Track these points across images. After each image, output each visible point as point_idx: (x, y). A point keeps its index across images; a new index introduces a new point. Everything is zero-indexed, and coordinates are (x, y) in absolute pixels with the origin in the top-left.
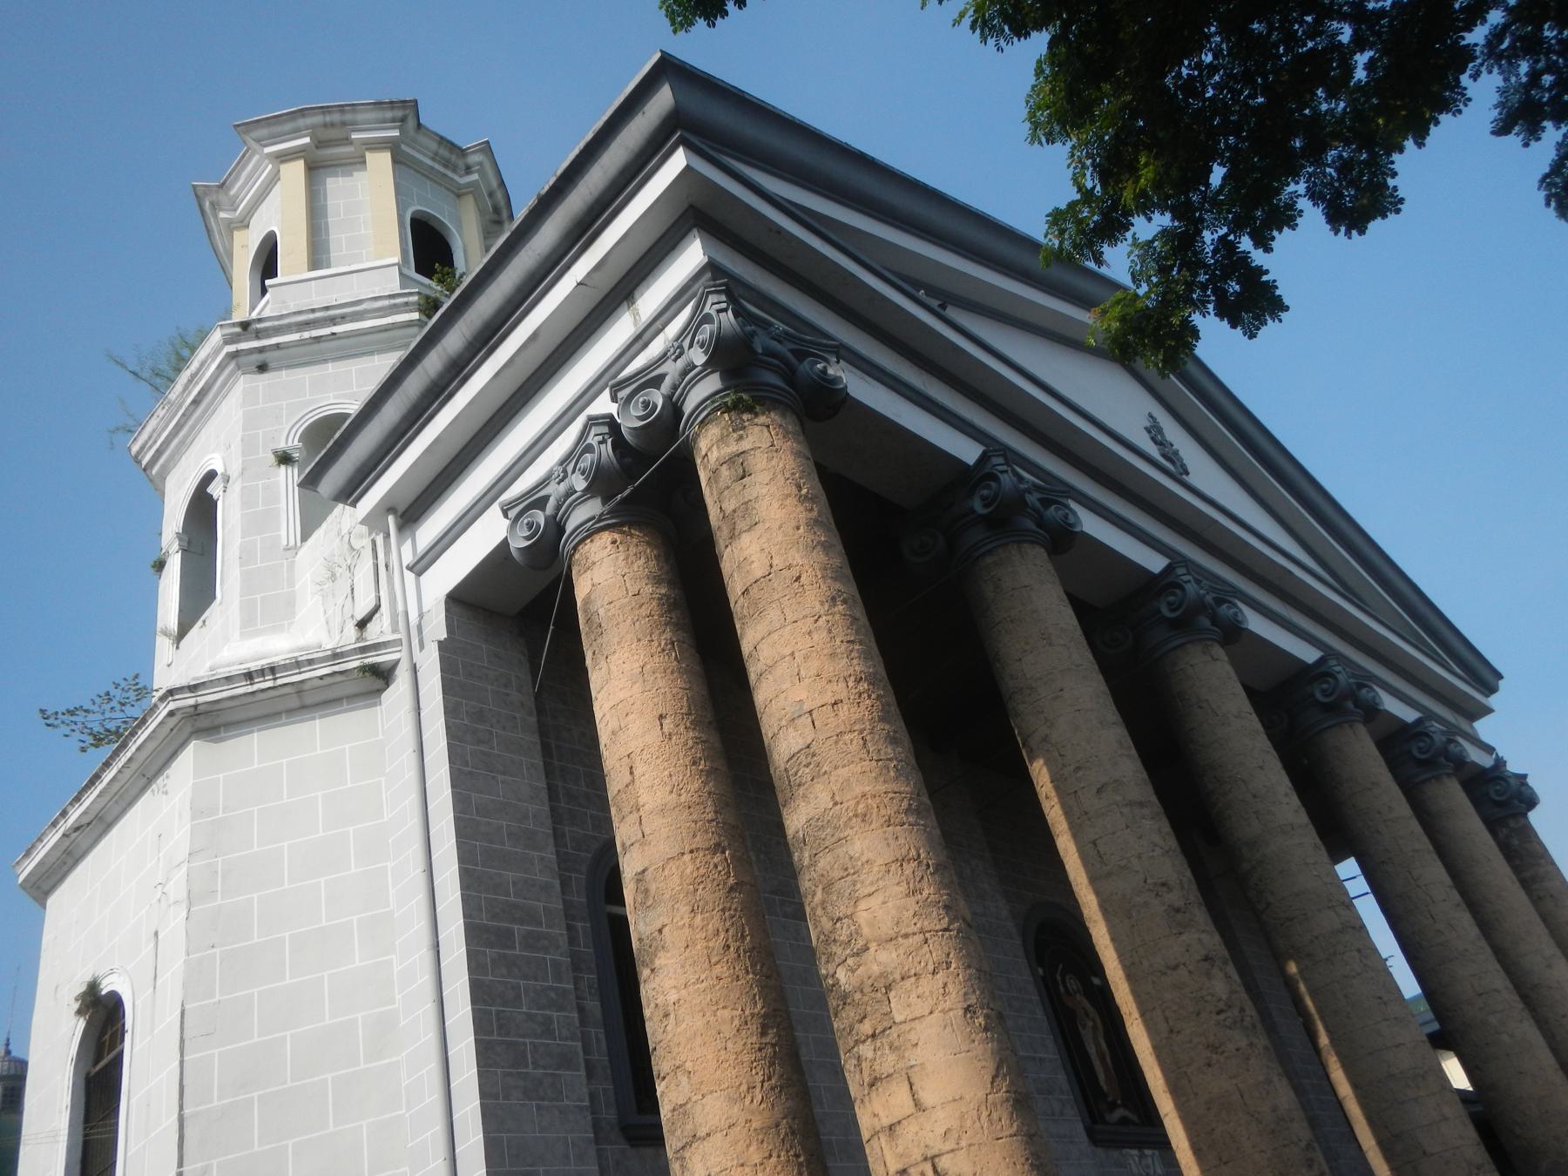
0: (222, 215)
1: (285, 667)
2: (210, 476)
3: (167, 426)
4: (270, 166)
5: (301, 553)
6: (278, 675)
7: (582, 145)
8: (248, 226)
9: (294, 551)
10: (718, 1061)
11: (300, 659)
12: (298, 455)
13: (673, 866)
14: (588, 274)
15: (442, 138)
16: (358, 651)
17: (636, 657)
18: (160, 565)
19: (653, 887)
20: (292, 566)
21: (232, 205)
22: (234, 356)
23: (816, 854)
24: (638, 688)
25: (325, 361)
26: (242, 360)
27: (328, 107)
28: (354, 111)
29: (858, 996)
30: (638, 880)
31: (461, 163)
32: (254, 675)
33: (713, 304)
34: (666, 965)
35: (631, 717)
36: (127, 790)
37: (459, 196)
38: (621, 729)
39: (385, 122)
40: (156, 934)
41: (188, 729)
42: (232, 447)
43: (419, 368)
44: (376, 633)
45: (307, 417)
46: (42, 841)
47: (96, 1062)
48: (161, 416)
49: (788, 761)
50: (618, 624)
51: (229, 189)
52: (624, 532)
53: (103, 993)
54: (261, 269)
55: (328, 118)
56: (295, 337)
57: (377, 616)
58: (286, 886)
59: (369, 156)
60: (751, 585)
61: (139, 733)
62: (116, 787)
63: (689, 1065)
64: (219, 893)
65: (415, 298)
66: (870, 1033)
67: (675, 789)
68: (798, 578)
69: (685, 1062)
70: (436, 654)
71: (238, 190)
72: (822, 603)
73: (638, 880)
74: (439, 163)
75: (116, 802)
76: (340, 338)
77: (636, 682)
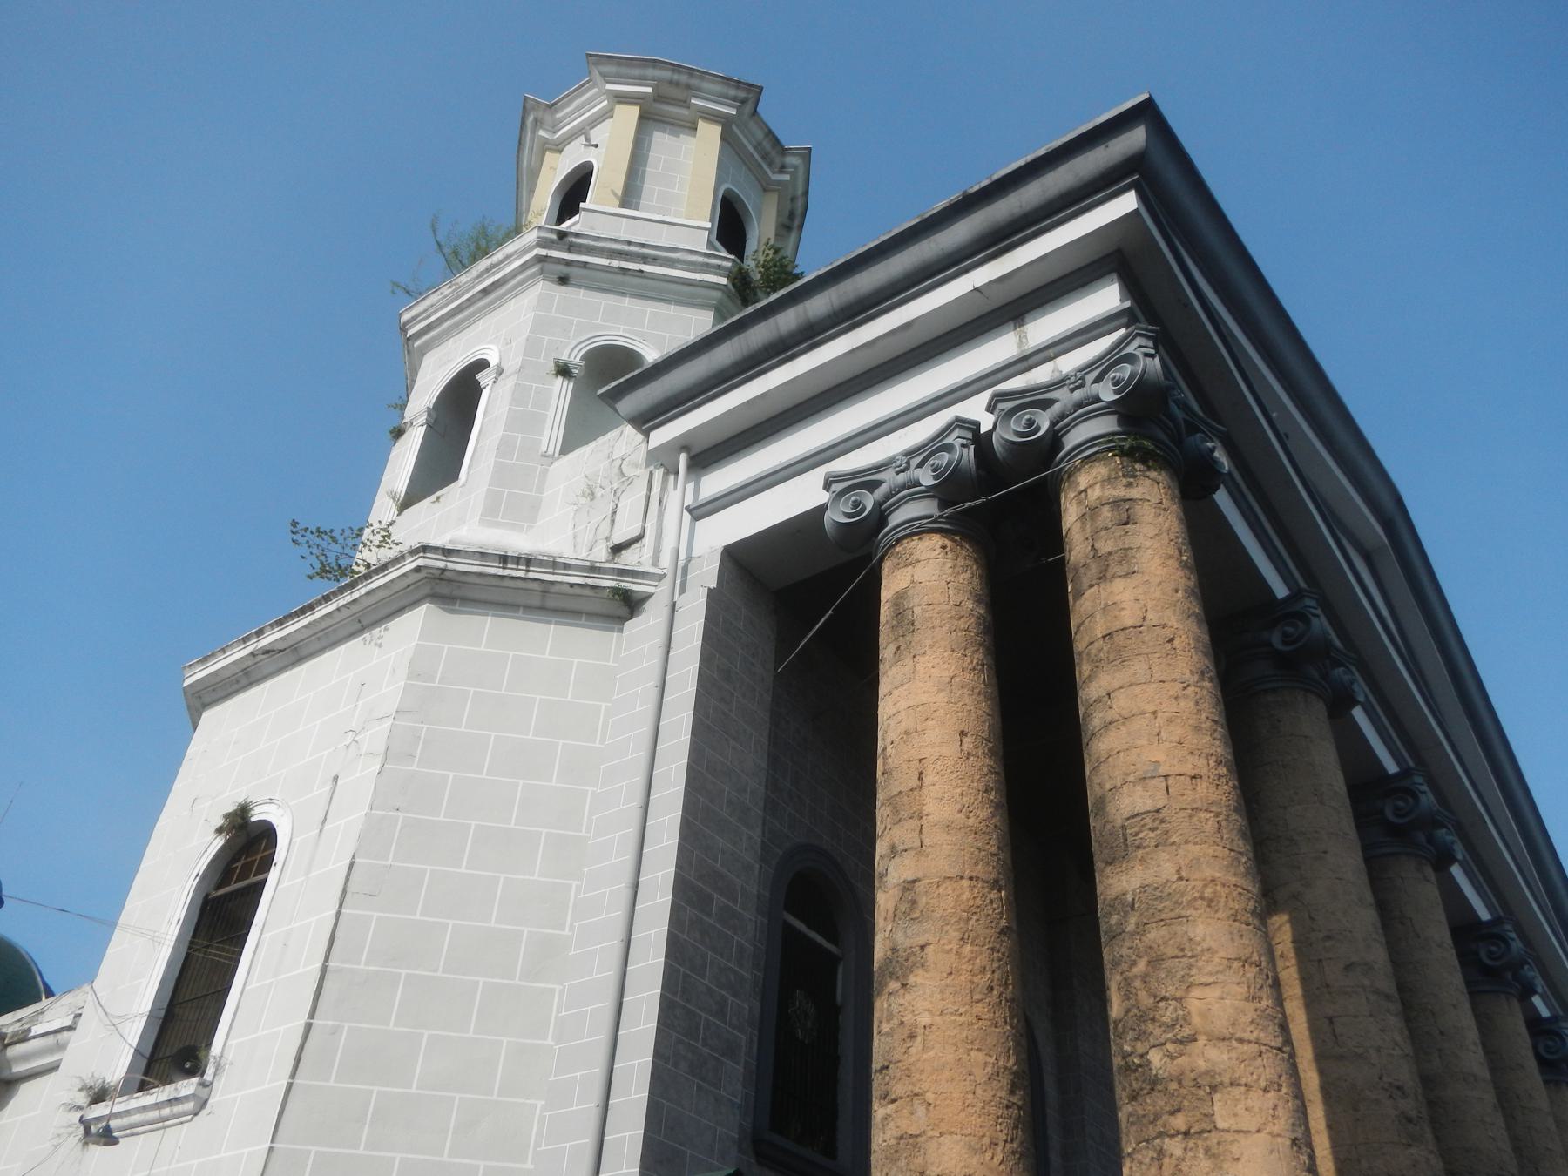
0: (542, 133)
1: (541, 563)
2: (482, 365)
3: (447, 305)
4: (606, 102)
5: (556, 464)
6: (531, 568)
7: (1030, 158)
8: (560, 151)
9: (551, 460)
10: (964, 1103)
11: (558, 560)
12: (577, 371)
13: (948, 888)
14: (990, 282)
15: (770, 132)
16: (616, 572)
17: (946, 666)
18: (398, 433)
19: (923, 901)
20: (544, 473)
21: (553, 127)
22: (541, 259)
23: (1146, 924)
24: (943, 697)
25: (624, 294)
26: (549, 266)
27: (681, 66)
28: (702, 78)
29: (1173, 1086)
30: (905, 887)
31: (778, 160)
32: (509, 560)
33: (1140, 346)
34: (921, 984)
35: (930, 723)
36: (334, 630)
37: (765, 190)
38: (916, 732)
39: (727, 98)
40: (336, 778)
41: (426, 590)
42: (514, 344)
43: (771, 321)
44: (629, 559)
46: (225, 653)
47: (218, 887)
48: (445, 293)
49: (1128, 819)
50: (933, 627)
51: (556, 111)
52: (955, 541)
53: (253, 819)
54: (563, 193)
55: (676, 77)
56: (604, 262)
57: (637, 545)
58: (484, 776)
59: (701, 125)
60: (1117, 631)
61: (374, 579)
62: (329, 622)
63: (930, 1097)
64: (416, 760)
65: (729, 264)
66: (1183, 1128)
67: (964, 810)
68: (1171, 640)
69: (926, 1092)
70: (702, 600)
72: (1192, 673)
73: (905, 887)
74: (759, 153)
75: (319, 639)
76: (645, 277)
77: (942, 690)
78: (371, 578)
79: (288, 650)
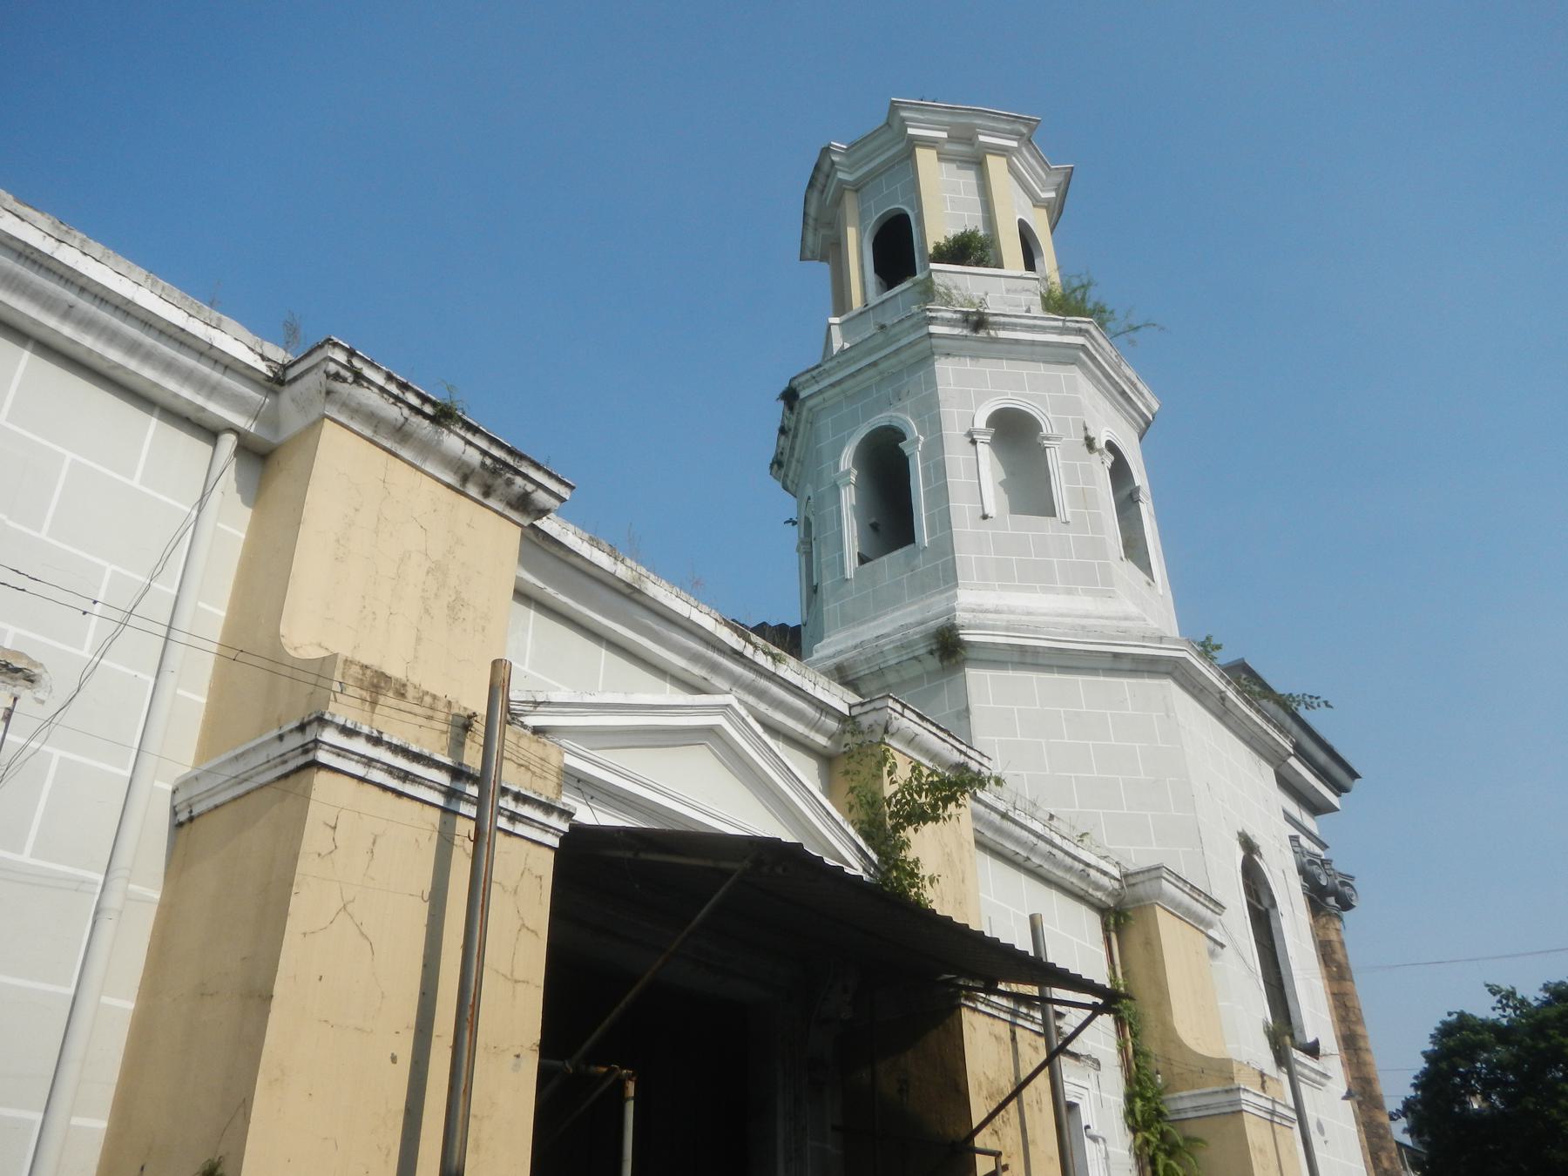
3: (1106, 362)
45: (1031, 407)
71: (1025, 156)
75: (1236, 722)
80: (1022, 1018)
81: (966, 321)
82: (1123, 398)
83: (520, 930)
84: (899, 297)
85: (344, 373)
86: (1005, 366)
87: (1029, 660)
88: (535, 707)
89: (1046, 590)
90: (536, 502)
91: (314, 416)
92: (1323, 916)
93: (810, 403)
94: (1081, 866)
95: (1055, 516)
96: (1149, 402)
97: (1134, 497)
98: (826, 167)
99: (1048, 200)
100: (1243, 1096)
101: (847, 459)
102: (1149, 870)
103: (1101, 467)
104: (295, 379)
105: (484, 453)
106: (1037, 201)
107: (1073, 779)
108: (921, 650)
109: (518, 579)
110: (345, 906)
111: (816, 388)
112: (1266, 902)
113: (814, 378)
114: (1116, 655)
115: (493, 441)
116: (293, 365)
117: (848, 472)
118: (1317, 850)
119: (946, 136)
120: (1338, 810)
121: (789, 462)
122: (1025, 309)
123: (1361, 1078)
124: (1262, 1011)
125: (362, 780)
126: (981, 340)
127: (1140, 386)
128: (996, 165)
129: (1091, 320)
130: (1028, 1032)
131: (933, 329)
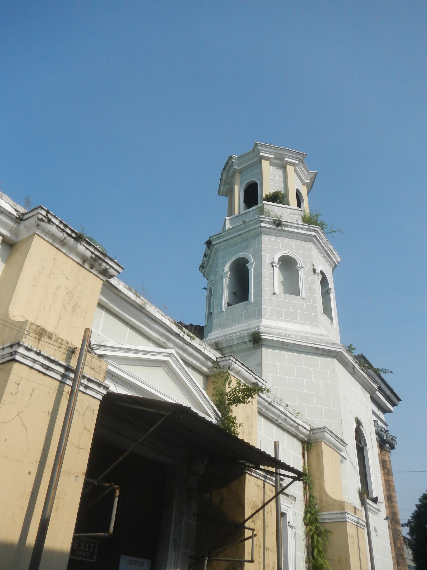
3: (323, 242)
71: (301, 167)
75: (358, 377)
78: (372, 380)
79: (354, 371)
80: (268, 479)
81: (274, 223)
82: (328, 256)
83: (83, 429)
84: (251, 212)
85: (44, 219)
86: (287, 240)
87: (285, 347)
88: (100, 347)
89: (293, 322)
90: (109, 272)
91: (32, 233)
92: (385, 451)
93: (216, 246)
94: (296, 425)
95: (299, 296)
96: (337, 258)
97: (329, 291)
98: (230, 163)
99: (308, 183)
100: (347, 515)
101: (227, 268)
102: (321, 428)
103: (318, 280)
104: (26, 219)
105: (92, 253)
106: (304, 183)
107: (297, 392)
108: (247, 340)
109: (100, 299)
110: (18, 414)
111: (218, 241)
112: (363, 444)
113: (218, 237)
114: (317, 348)
115: (96, 249)
116: (26, 214)
117: (227, 273)
118: (384, 426)
119: (274, 157)
120: (392, 412)
121: (206, 267)
122: (296, 220)
123: (393, 512)
124: (358, 484)
125: (31, 368)
126: (279, 230)
127: (334, 252)
128: (290, 169)
129: (319, 227)
130: (270, 485)
131: (262, 224)
